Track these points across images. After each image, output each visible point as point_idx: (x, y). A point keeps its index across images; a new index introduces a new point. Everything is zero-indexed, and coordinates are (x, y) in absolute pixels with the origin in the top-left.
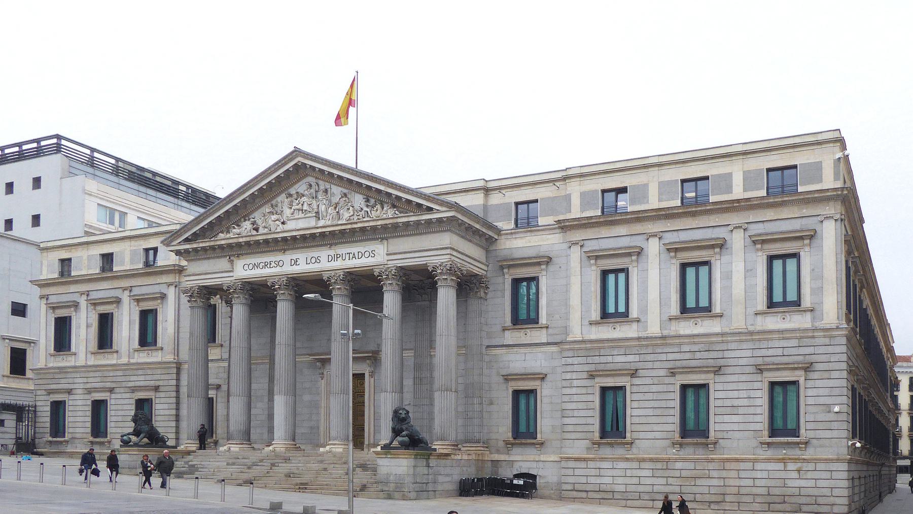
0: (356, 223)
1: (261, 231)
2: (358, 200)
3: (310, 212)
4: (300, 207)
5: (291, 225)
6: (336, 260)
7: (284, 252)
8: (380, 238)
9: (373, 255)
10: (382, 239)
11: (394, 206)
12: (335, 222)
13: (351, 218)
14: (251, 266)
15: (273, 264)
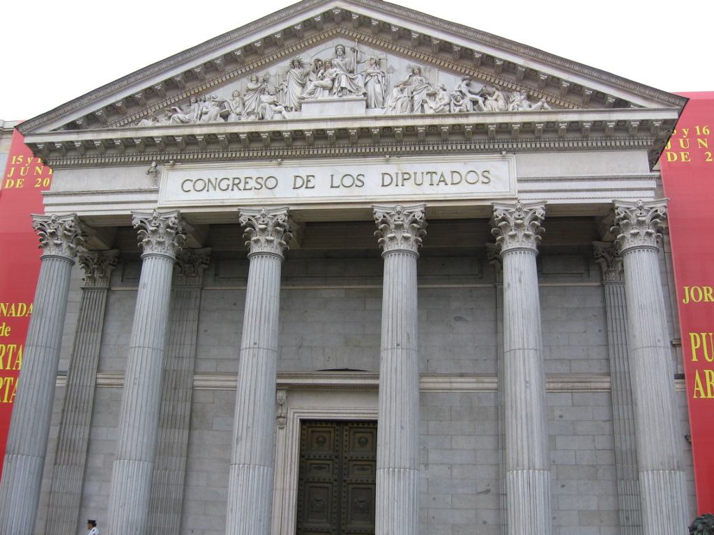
0: (467, 115)
1: (232, 118)
2: (449, 83)
3: (350, 91)
4: (327, 82)
5: (309, 111)
6: (400, 184)
7: (280, 164)
8: (505, 149)
9: (486, 180)
10: (508, 151)
11: (529, 98)
12: (407, 113)
13: (447, 108)
14: (200, 185)
15: (252, 184)
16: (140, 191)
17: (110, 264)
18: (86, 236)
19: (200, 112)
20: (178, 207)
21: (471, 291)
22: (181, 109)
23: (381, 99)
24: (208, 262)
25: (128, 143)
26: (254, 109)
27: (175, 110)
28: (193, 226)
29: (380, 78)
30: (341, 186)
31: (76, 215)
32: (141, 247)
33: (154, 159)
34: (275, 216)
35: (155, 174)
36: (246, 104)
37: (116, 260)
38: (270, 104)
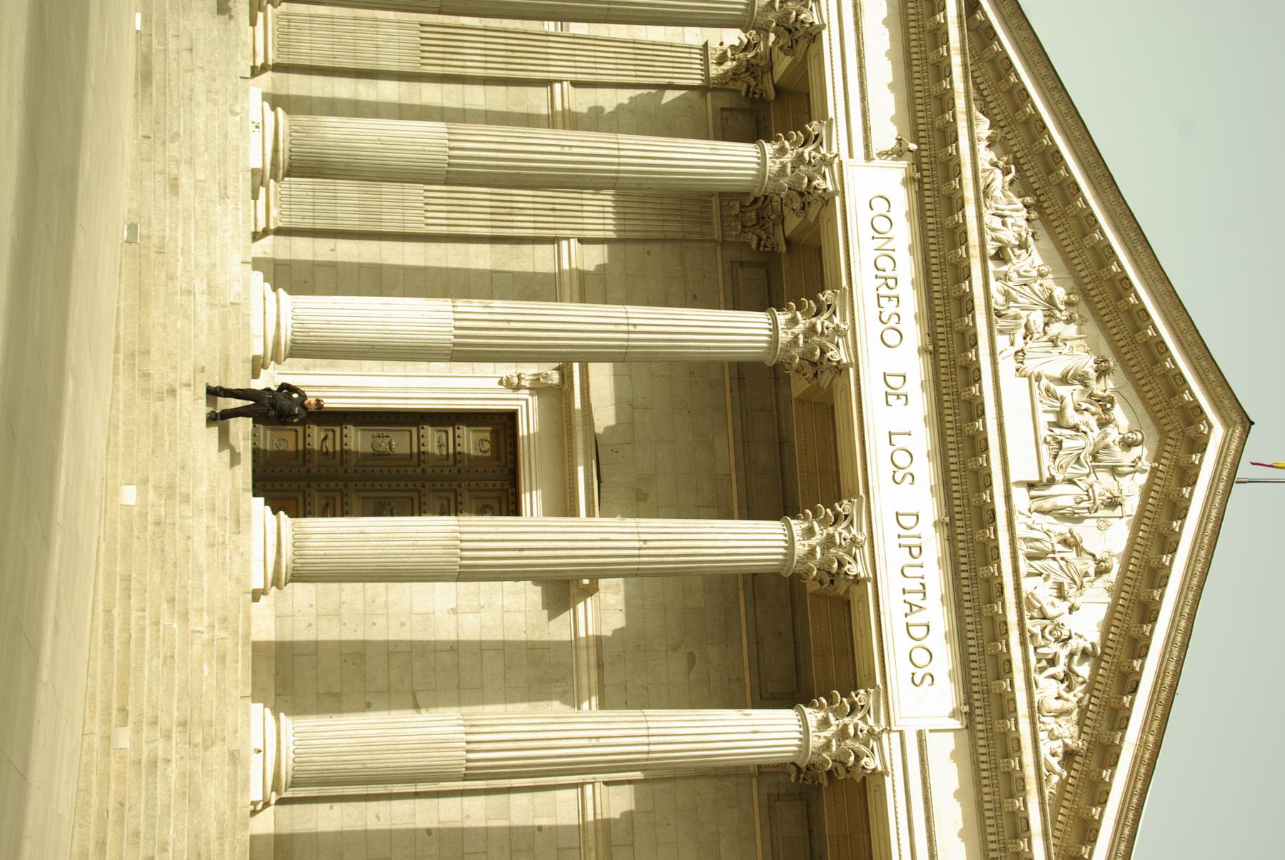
16: (866, 130)
17: (749, 87)
18: (792, 47)
19: (1005, 213)
20: (843, 193)
21: (738, 679)
22: (1011, 182)
23: (1047, 505)
24: (761, 249)
25: (945, 101)
26: (1016, 302)
27: (1009, 172)
28: (817, 218)
29: (1084, 504)
30: (893, 448)
31: (824, 29)
32: (777, 139)
33: (925, 173)
34: (837, 346)
35: (898, 153)
36: (1026, 288)
37: (756, 96)
38: (1026, 326)
